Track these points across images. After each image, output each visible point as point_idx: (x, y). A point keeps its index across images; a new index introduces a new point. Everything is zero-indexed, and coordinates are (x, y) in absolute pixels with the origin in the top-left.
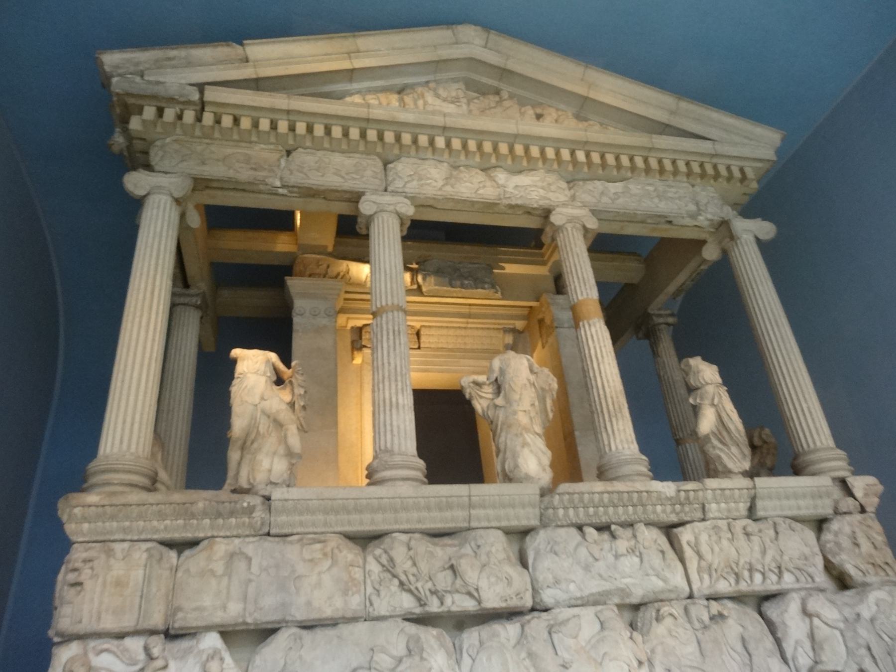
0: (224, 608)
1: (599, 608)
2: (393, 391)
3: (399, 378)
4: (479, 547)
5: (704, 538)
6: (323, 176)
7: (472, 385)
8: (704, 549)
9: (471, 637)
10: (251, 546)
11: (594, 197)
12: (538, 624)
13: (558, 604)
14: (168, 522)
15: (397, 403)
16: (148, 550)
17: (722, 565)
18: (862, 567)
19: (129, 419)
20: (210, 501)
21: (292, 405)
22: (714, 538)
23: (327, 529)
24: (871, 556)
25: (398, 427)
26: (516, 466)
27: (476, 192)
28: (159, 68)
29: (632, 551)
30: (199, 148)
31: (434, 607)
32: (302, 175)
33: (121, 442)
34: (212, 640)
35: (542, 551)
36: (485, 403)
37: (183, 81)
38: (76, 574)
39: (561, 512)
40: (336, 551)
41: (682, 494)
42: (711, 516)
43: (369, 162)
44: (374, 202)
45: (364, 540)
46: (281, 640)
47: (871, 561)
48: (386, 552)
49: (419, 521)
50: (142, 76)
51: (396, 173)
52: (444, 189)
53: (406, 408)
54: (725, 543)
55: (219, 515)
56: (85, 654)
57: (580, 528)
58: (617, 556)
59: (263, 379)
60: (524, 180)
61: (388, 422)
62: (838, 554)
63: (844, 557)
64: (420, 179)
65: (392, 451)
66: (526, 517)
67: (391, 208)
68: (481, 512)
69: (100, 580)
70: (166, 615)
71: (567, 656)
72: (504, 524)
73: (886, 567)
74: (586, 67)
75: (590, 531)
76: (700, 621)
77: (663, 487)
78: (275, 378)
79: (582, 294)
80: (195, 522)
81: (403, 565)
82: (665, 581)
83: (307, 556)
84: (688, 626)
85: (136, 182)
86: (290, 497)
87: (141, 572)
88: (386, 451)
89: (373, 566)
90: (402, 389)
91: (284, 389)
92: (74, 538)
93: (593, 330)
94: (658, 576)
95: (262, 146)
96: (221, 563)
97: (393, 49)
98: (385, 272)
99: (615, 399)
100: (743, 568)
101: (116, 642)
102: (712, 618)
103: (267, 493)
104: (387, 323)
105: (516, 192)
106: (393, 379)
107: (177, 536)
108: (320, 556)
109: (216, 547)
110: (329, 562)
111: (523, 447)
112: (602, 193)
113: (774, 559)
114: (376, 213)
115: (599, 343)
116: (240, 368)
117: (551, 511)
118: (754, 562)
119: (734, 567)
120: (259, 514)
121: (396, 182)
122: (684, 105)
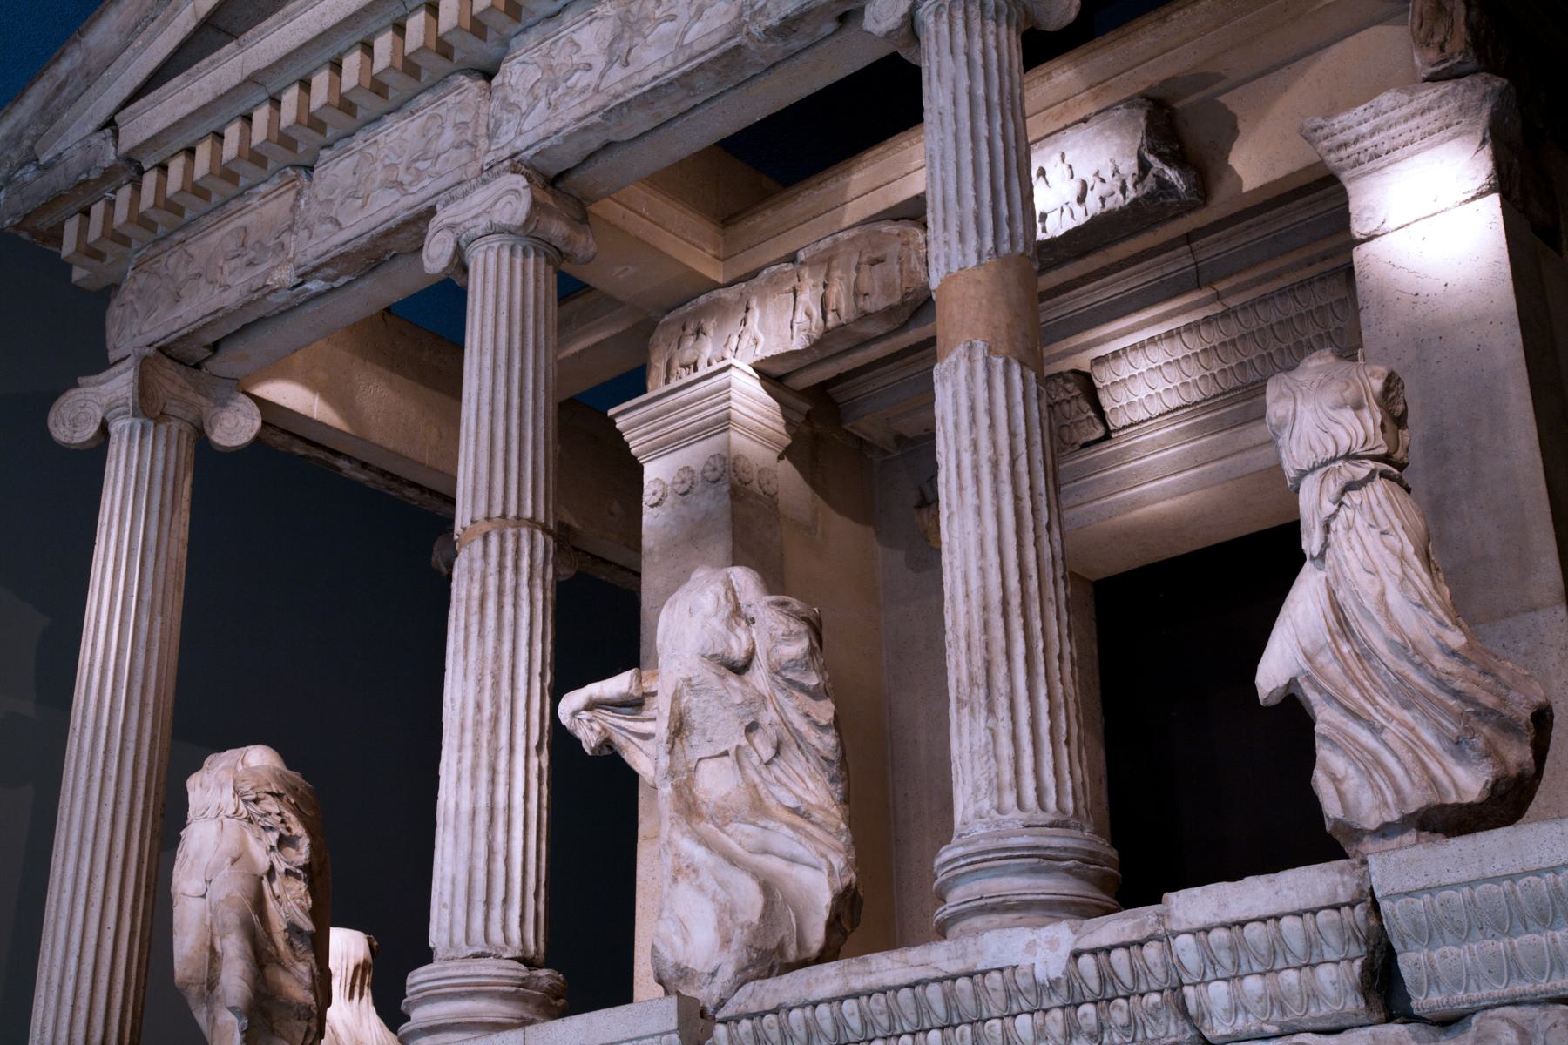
7: (585, 715)
27: (681, 47)
28: (51, 123)
32: (329, 226)
37: (91, 127)
41: (1087, 962)
43: (450, 99)
51: (505, 99)
67: (483, 222)
77: (1031, 947)
90: (475, 768)
95: (263, 188)
111: (675, 880)
114: (459, 252)
121: (504, 129)
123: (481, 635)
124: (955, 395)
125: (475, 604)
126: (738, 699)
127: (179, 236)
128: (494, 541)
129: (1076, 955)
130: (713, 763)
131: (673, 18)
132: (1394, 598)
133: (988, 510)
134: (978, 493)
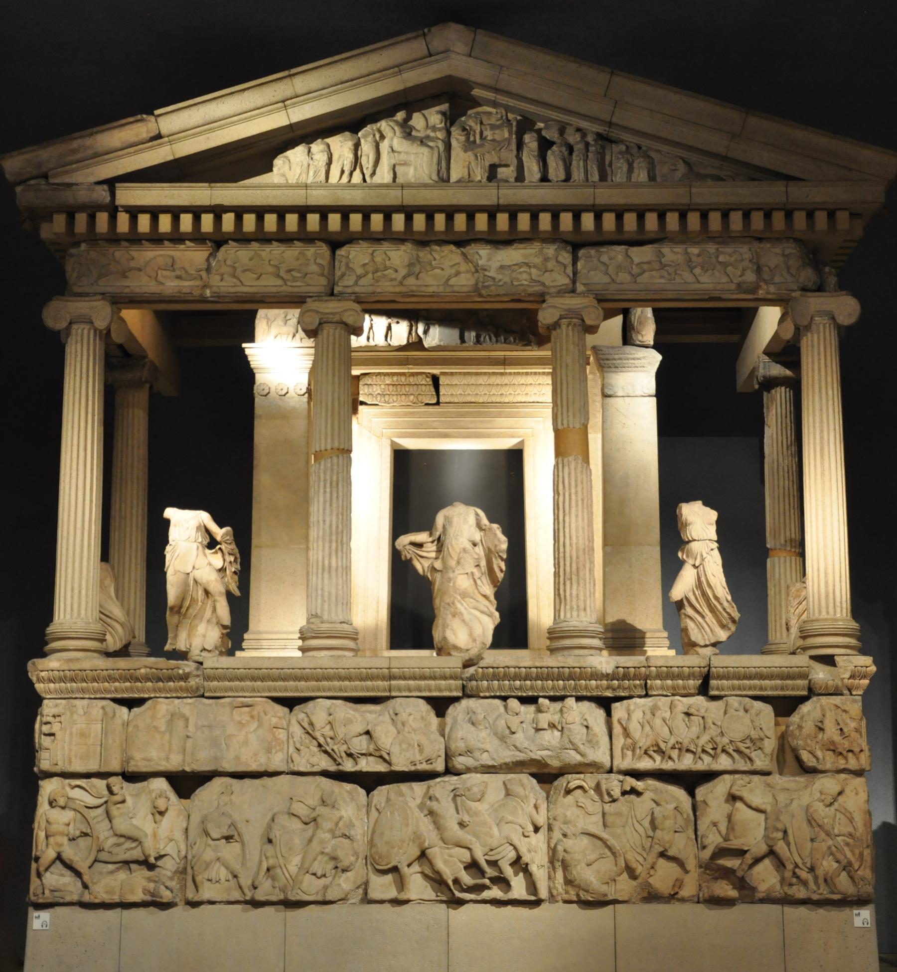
0: (168, 759)
1: (510, 776)
2: (327, 552)
3: (334, 538)
4: (396, 714)
5: (637, 715)
6: (258, 278)
7: (408, 547)
8: (634, 728)
9: (381, 793)
10: (188, 707)
11: (606, 273)
12: (442, 787)
13: (468, 770)
14: (117, 684)
15: (330, 566)
16: (103, 708)
17: (648, 743)
18: (819, 754)
19: (76, 586)
20: (151, 668)
21: (222, 570)
22: (649, 715)
23: (255, 694)
24: (832, 742)
25: (330, 594)
26: (445, 638)
29: (552, 726)
30: (117, 254)
31: (348, 766)
32: (235, 280)
33: (72, 609)
34: (161, 784)
35: (459, 721)
36: (427, 564)
37: (92, 179)
38: (49, 726)
39: (485, 682)
40: (262, 714)
42: (654, 693)
44: (317, 312)
45: (290, 703)
46: (217, 784)
47: (832, 748)
48: (308, 716)
49: (341, 690)
50: (45, 176)
51: (347, 265)
52: (405, 282)
53: (340, 570)
54: (658, 722)
55: (159, 680)
56: (63, 788)
57: (504, 699)
58: (538, 730)
59: (195, 545)
60: (512, 255)
61: (320, 586)
62: (797, 738)
63: (800, 742)
64: (377, 271)
65: (321, 617)
66: (451, 689)
68: (402, 683)
69: (68, 732)
70: (122, 762)
71: (466, 818)
72: (424, 694)
73: (850, 754)
74: (612, 73)
75: (514, 703)
76: (609, 794)
78: (208, 540)
79: (562, 424)
80: (139, 684)
81: (323, 730)
82: (582, 755)
83: (237, 718)
84: (597, 798)
85: (56, 314)
86: (220, 666)
87: (99, 726)
88: (316, 616)
89: (297, 730)
91: (216, 553)
92: (43, 695)
93: (566, 471)
94: (576, 750)
96: (163, 720)
97: (342, 83)
98: (327, 406)
99: (574, 559)
100: (673, 748)
101: (85, 780)
102: (624, 793)
103: (201, 660)
104: (325, 473)
105: (500, 277)
106: (327, 538)
107: (125, 696)
108: (248, 718)
109: (158, 707)
110: (255, 725)
111: (454, 616)
112: (619, 268)
113: (712, 740)
114: (320, 324)
115: (570, 489)
116: (174, 534)
117: (474, 683)
118: (686, 742)
119: (663, 746)
120: (193, 682)
121: (346, 278)
122: (754, 122)
123: (337, 497)
124: (569, 473)
125: (334, 484)
126: (476, 557)
127: (125, 244)
128: (341, 457)
129: (617, 667)
130: (462, 576)
131: (443, 269)
132: (718, 585)
133: (580, 516)
134: (577, 511)
